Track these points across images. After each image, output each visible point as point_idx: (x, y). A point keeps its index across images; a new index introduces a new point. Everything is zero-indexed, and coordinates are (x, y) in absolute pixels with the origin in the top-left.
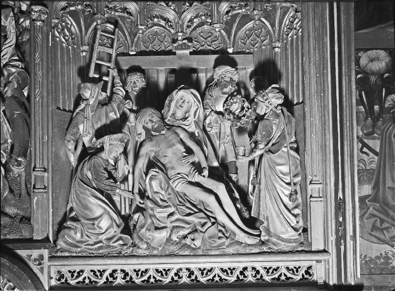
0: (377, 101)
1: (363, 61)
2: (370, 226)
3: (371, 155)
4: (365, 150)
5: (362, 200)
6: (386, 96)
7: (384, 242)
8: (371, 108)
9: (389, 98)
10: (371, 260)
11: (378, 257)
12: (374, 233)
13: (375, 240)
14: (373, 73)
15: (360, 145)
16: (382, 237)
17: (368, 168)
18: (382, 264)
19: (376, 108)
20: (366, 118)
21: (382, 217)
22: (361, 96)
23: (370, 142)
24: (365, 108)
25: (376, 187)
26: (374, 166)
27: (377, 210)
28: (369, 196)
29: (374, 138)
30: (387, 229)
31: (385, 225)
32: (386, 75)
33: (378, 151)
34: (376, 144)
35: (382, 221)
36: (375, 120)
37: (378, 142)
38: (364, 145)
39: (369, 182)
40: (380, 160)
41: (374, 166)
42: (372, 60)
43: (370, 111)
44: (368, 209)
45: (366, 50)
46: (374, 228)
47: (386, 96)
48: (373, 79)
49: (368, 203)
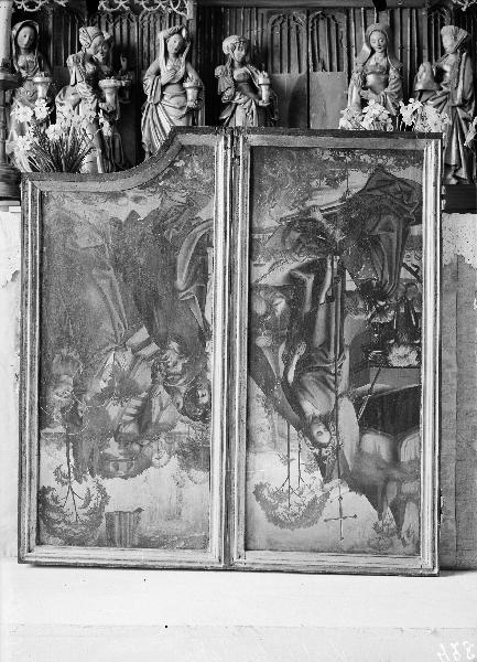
1: (413, 356)
3: (409, 264)
5: (419, 221)
7: (402, 181)
8: (407, 310)
10: (413, 163)
14: (405, 344)
23: (409, 276)
25: (406, 233)
29: (406, 280)
32: (392, 341)
34: (404, 274)
35: (402, 200)
37: (402, 276)
38: (415, 274)
40: (401, 259)
43: (409, 307)
45: (409, 367)
46: (409, 194)
49: (413, 217)
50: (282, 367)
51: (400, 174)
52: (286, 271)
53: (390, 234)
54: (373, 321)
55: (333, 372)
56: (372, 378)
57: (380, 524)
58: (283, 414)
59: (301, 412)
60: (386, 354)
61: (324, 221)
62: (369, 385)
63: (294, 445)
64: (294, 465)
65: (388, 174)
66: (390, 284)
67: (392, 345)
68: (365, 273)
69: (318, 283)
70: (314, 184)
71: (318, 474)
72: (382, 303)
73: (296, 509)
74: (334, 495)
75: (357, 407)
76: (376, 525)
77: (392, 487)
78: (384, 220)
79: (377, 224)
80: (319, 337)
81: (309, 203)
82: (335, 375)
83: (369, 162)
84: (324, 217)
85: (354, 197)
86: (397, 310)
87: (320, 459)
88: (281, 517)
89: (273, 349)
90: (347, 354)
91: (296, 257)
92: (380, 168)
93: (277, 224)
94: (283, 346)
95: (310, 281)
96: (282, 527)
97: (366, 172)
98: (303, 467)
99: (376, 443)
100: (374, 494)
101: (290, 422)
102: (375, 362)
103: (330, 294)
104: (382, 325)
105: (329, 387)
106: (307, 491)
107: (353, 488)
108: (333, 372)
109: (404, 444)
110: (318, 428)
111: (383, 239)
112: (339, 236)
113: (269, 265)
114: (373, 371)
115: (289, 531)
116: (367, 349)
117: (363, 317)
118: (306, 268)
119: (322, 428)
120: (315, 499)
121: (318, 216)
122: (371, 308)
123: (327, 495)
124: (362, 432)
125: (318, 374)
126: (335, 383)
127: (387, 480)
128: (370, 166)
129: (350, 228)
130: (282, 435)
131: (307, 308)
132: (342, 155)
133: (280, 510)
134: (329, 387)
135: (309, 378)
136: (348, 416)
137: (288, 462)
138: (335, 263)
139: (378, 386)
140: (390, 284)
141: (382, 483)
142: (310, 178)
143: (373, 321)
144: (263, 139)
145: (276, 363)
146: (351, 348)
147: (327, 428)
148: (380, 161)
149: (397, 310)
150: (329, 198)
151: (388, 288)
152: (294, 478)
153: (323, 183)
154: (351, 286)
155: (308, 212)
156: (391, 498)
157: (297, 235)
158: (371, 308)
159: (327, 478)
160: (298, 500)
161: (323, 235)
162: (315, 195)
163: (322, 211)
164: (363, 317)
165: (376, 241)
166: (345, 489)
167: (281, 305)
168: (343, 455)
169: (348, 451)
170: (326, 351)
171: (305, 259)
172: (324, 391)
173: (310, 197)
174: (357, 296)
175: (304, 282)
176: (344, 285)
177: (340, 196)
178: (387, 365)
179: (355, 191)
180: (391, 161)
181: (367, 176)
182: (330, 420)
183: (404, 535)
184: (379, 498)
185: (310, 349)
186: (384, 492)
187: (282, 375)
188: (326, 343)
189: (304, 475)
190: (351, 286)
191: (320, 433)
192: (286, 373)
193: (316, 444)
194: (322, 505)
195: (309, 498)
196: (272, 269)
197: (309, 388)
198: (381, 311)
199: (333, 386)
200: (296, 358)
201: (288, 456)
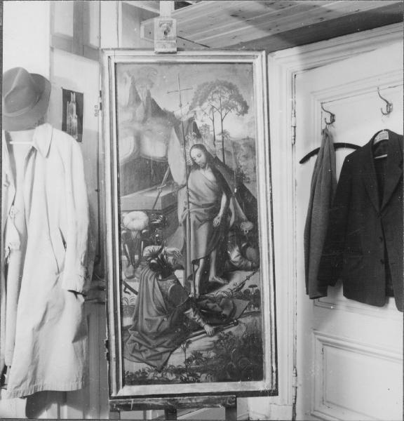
0: (138, 251)
2: (132, 349)
3: (132, 293)
4: (127, 290)
6: (144, 248)
7: (141, 361)
8: (133, 258)
9: (147, 249)
11: (137, 373)
12: (134, 355)
13: (134, 359)
14: (134, 230)
15: (123, 286)
16: (141, 357)
17: (130, 304)
18: (141, 377)
19: (136, 257)
20: (128, 266)
21: (141, 342)
22: (124, 247)
23: (131, 284)
24: (127, 257)
25: (136, 318)
26: (134, 302)
27: (137, 337)
28: (131, 326)
29: (135, 281)
30: (144, 351)
31: (143, 348)
32: (144, 231)
33: (137, 290)
35: (141, 345)
36: (135, 267)
38: (127, 286)
39: (131, 315)
40: (139, 298)
41: (134, 302)
42: (133, 220)
44: (130, 335)
45: (129, 211)
46: (134, 350)
47: (144, 248)
48: (134, 234)
49: (130, 331)
50: (231, 207)
51: (145, 365)
52: (231, 283)
53: (149, 318)
54: (160, 247)
55: (191, 205)
56: (160, 201)
57: (148, 88)
58: (230, 171)
59: (215, 172)
60: (150, 220)
61: (203, 324)
62: (162, 195)
63: (219, 146)
64: (218, 130)
65: (151, 365)
66: (147, 277)
67: (146, 228)
68: (169, 284)
69: (205, 273)
70: (212, 354)
71: (199, 125)
72: (153, 261)
73: (216, 96)
74: (186, 108)
75: (170, 177)
76: (152, 85)
77: (140, 115)
78: (155, 329)
79: (160, 325)
80: (203, 232)
81: (215, 338)
82: (189, 202)
83: (168, 374)
84: (203, 328)
85: (179, 345)
86: (140, 256)
87: (199, 136)
88: (227, 89)
89: (239, 220)
90: (180, 220)
91: (225, 295)
92: (160, 370)
93: (240, 320)
94: (232, 222)
95: (212, 276)
96: (226, 82)
97: (170, 366)
98: (211, 129)
99: (154, 150)
100: (156, 111)
101: (223, 164)
102: (158, 213)
103: (196, 267)
104: (153, 244)
105: (192, 192)
106: (207, 111)
107: (172, 115)
108: (191, 205)
109: (131, 151)
110: (201, 159)
111: (154, 313)
112: (190, 313)
113: (246, 287)
114: (159, 207)
115: (220, 79)
116: (164, 224)
117: (168, 249)
118: (216, 286)
119: (198, 160)
120: (201, 104)
121: (208, 329)
122: (162, 256)
123: (191, 108)
124: (166, 158)
125: (204, 202)
126: (188, 195)
127: (145, 121)
128: (167, 371)
129: (183, 318)
130: (229, 153)
131: (213, 254)
132: (190, 378)
133: (227, 95)
134: (192, 192)
135: (210, 199)
136: (177, 170)
137: (223, 132)
138: (192, 291)
139: (154, 195)
140: (147, 277)
141: (148, 120)
142: (216, 358)
143: (160, 247)
144: (254, 387)
145: (235, 208)
146: (177, 224)
147: (193, 160)
148: (159, 375)
149: (140, 256)
150: (199, 343)
151: (149, 273)
152: (218, 120)
153: (205, 354)
154: (179, 274)
155: (216, 332)
156: (140, 109)
157: (224, 312)
158: (162, 256)
159: (191, 120)
160: (214, 104)
161: (203, 314)
162: (210, 345)
163: (205, 332)
164: (168, 249)
165: (162, 311)
166: (178, 113)
167: (234, 255)
168: (179, 137)
169: (175, 142)
170: (197, 221)
171: (216, 294)
172: (196, 188)
173: (215, 343)
174: (173, 267)
175: (217, 274)
176: (186, 274)
177: (190, 346)
178: (147, 212)
179: (179, 350)
180: (150, 376)
181: (170, 362)
182: (192, 167)
183: (129, 79)
184: (150, 107)
185: (211, 221)
186: (146, 112)
187: (231, 200)
188: (196, 227)
189: (209, 123)
190: (179, 274)
191: (199, 156)
192: (228, 203)
193: (202, 147)
194: (195, 100)
195: (205, 105)
196: (243, 284)
197: (209, 190)
198: (154, 255)
199: (190, 193)
200: (221, 214)
201: (223, 137)
